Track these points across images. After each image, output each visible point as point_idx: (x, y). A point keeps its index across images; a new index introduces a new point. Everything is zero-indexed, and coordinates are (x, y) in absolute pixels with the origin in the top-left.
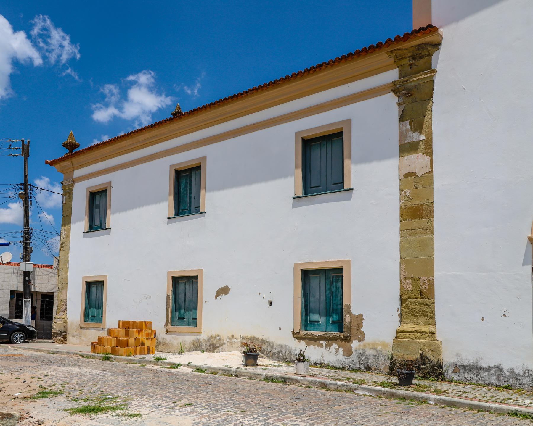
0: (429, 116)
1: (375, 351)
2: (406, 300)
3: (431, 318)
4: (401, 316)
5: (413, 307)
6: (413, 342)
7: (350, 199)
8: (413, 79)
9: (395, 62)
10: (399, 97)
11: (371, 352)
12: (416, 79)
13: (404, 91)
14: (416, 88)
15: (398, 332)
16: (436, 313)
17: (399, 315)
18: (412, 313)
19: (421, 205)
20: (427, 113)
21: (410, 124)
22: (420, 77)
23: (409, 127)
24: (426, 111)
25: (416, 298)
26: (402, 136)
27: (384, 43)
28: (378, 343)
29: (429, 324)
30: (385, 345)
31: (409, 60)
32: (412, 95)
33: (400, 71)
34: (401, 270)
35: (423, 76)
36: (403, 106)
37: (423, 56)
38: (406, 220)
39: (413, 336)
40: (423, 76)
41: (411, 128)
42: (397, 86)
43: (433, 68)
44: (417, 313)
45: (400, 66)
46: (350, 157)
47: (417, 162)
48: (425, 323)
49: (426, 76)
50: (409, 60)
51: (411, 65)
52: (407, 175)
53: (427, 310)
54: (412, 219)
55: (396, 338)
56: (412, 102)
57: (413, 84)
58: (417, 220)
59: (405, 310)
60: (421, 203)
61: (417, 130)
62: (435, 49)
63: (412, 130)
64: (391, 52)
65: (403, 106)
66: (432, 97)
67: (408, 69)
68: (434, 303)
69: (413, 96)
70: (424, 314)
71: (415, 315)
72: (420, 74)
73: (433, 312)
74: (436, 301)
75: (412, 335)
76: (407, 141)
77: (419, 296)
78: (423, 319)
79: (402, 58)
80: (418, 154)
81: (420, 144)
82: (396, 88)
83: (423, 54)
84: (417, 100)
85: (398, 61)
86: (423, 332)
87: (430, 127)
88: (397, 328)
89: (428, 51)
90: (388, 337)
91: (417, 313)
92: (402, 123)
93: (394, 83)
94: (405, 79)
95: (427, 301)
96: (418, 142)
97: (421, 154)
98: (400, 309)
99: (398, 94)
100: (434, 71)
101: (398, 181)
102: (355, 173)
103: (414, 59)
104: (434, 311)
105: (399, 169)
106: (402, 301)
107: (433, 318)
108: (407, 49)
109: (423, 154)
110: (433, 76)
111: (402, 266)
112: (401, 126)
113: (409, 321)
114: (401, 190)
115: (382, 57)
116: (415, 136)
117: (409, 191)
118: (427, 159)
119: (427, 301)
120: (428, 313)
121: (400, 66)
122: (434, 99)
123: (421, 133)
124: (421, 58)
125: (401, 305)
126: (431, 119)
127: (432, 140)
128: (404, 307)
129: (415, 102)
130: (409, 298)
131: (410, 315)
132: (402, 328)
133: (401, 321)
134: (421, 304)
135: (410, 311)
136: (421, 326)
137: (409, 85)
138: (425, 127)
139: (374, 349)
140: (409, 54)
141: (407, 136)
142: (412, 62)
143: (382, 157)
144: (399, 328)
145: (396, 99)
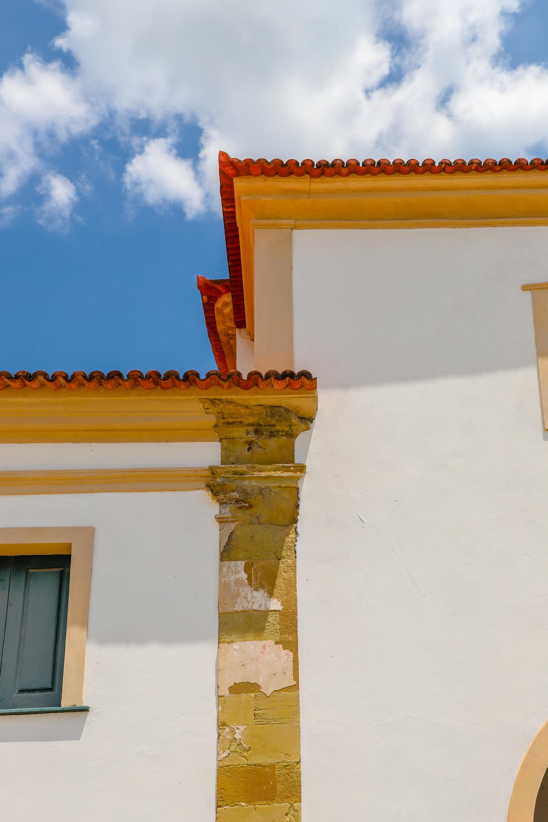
0: (290, 561)
7: (76, 736)
8: (257, 474)
9: (216, 426)
10: (222, 503)
12: (263, 474)
13: (235, 495)
14: (261, 493)
19: (272, 766)
20: (284, 553)
21: (247, 569)
22: (272, 473)
23: (244, 576)
24: (282, 549)
26: (226, 592)
27: (203, 376)
31: (248, 433)
32: (250, 507)
33: (224, 449)
35: (279, 474)
36: (231, 527)
37: (278, 432)
38: (234, 803)
40: (279, 474)
41: (249, 579)
42: (219, 480)
43: (297, 461)
45: (226, 438)
46: (85, 623)
47: (260, 659)
49: (285, 474)
50: (248, 433)
51: (250, 444)
52: (237, 689)
54: (249, 802)
56: (252, 523)
57: (254, 483)
58: (262, 806)
60: (270, 761)
61: (262, 586)
62: (303, 426)
63: (250, 583)
64: (212, 401)
65: (231, 527)
66: (296, 522)
67: (242, 450)
69: (254, 509)
72: (275, 466)
76: (238, 608)
79: (233, 423)
80: (263, 643)
81: (270, 619)
82: (215, 484)
83: (278, 428)
84: (262, 520)
85: (223, 427)
87: (292, 584)
89: (290, 426)
92: (227, 563)
93: (213, 470)
94: (242, 468)
96: (265, 614)
97: (270, 643)
99: (221, 496)
100: (302, 468)
101: (214, 699)
102: (95, 665)
103: (257, 432)
105: (218, 671)
108: (246, 407)
109: (277, 643)
110: (298, 478)
112: (225, 569)
114: (221, 725)
115: (189, 406)
116: (257, 600)
117: (242, 728)
118: (286, 656)
121: (226, 438)
122: (300, 525)
123: (271, 594)
124: (272, 435)
126: (293, 568)
127: (295, 613)
129: (258, 522)
137: (246, 483)
138: (279, 581)
140: (251, 420)
141: (239, 595)
142: (252, 437)
143: (174, 634)
145: (214, 508)
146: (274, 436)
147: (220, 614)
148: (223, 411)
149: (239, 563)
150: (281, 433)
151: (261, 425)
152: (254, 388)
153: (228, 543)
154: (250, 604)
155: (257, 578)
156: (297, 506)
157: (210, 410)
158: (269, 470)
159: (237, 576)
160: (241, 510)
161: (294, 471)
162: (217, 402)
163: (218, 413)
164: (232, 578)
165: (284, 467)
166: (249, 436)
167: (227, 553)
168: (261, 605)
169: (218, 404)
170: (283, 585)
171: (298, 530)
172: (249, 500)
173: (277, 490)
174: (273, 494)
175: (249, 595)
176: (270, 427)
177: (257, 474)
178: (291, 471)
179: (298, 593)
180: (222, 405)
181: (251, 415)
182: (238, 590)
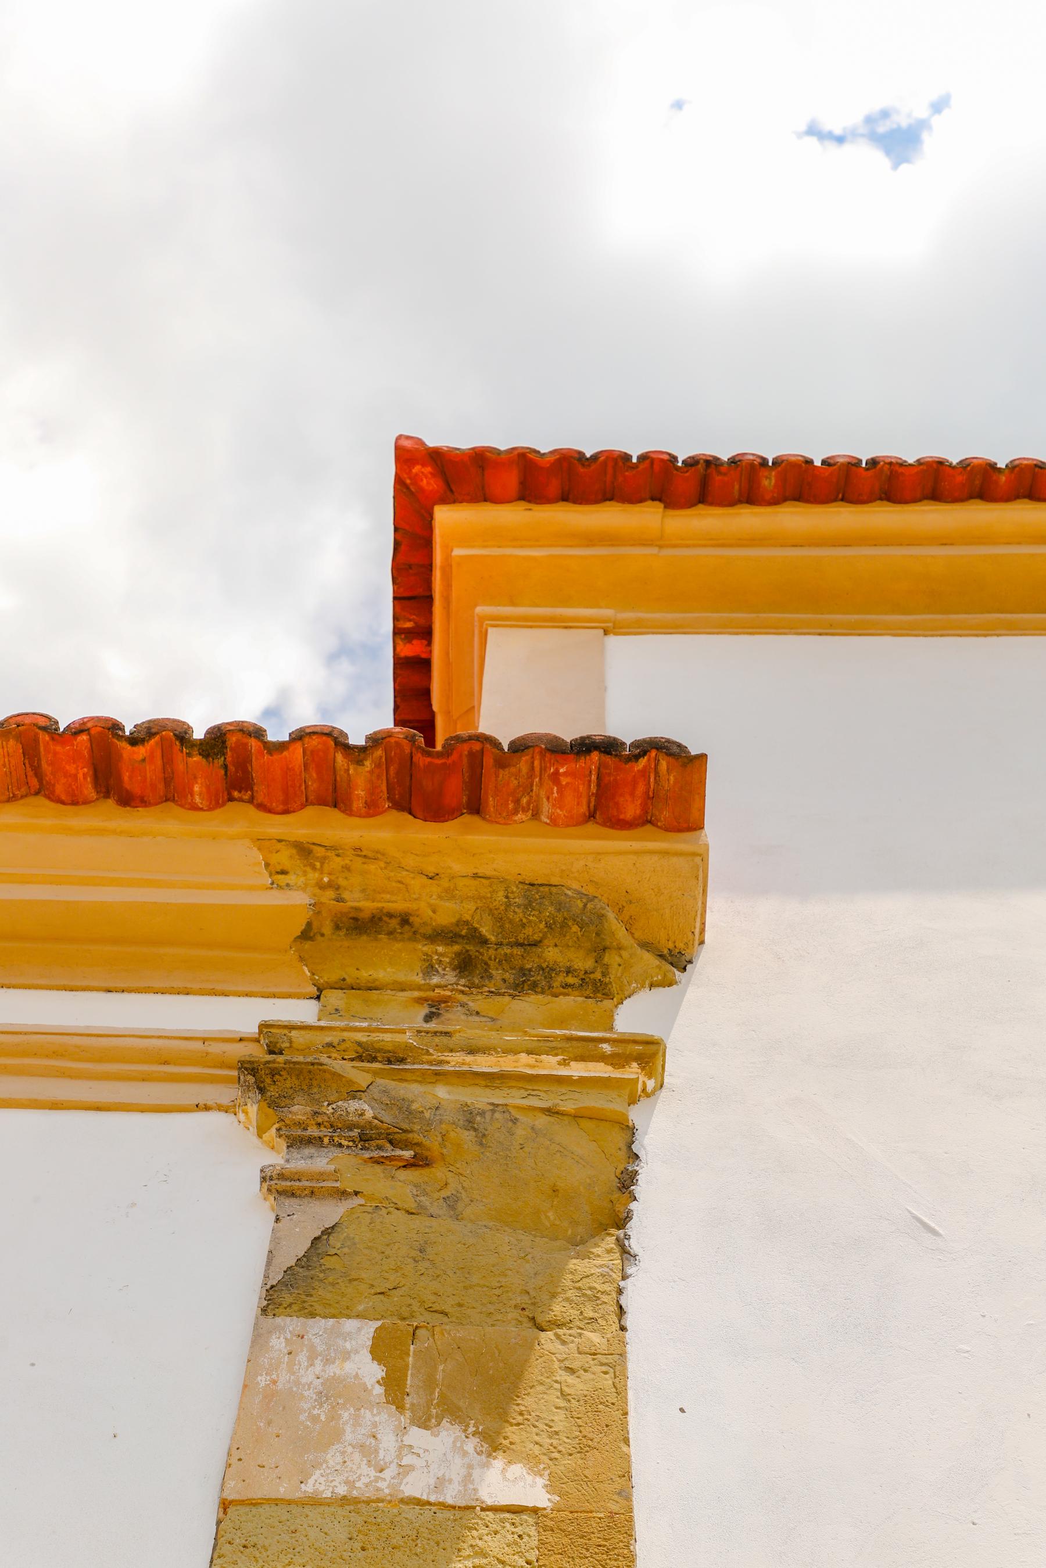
21: (382, 1349)
23: (372, 1372)
31: (430, 969)
32: (421, 1161)
37: (549, 971)
45: (342, 985)
49: (577, 1070)
50: (430, 969)
61: (453, 1412)
64: (304, 850)
69: (438, 1172)
76: (321, 1483)
83: (552, 954)
89: (600, 950)
92: (291, 1324)
99: (299, 1110)
103: (464, 965)
112: (278, 1343)
124: (524, 983)
127: (621, 1525)
146: (534, 987)
147: (225, 1505)
148: (342, 882)
149: (350, 1325)
150: (561, 979)
151: (485, 942)
152: (467, 818)
153: (305, 1261)
154: (387, 1474)
155: (430, 1383)
156: (627, 1182)
157: (291, 879)
158: (511, 1050)
159: (333, 1370)
160: (378, 1168)
161: (617, 1060)
162: (319, 852)
163: (322, 887)
164: (310, 1375)
165: (570, 1039)
166: (435, 980)
167: (293, 1290)
168: (440, 1483)
169: (323, 860)
170: (559, 1417)
171: (634, 1245)
172: (415, 1137)
173: (542, 1121)
174: (520, 1132)
175: (388, 1442)
176: (518, 951)
177: (456, 1061)
178: (603, 1058)
179: (635, 1450)
180: (337, 862)
181: (450, 894)
182: (333, 1417)
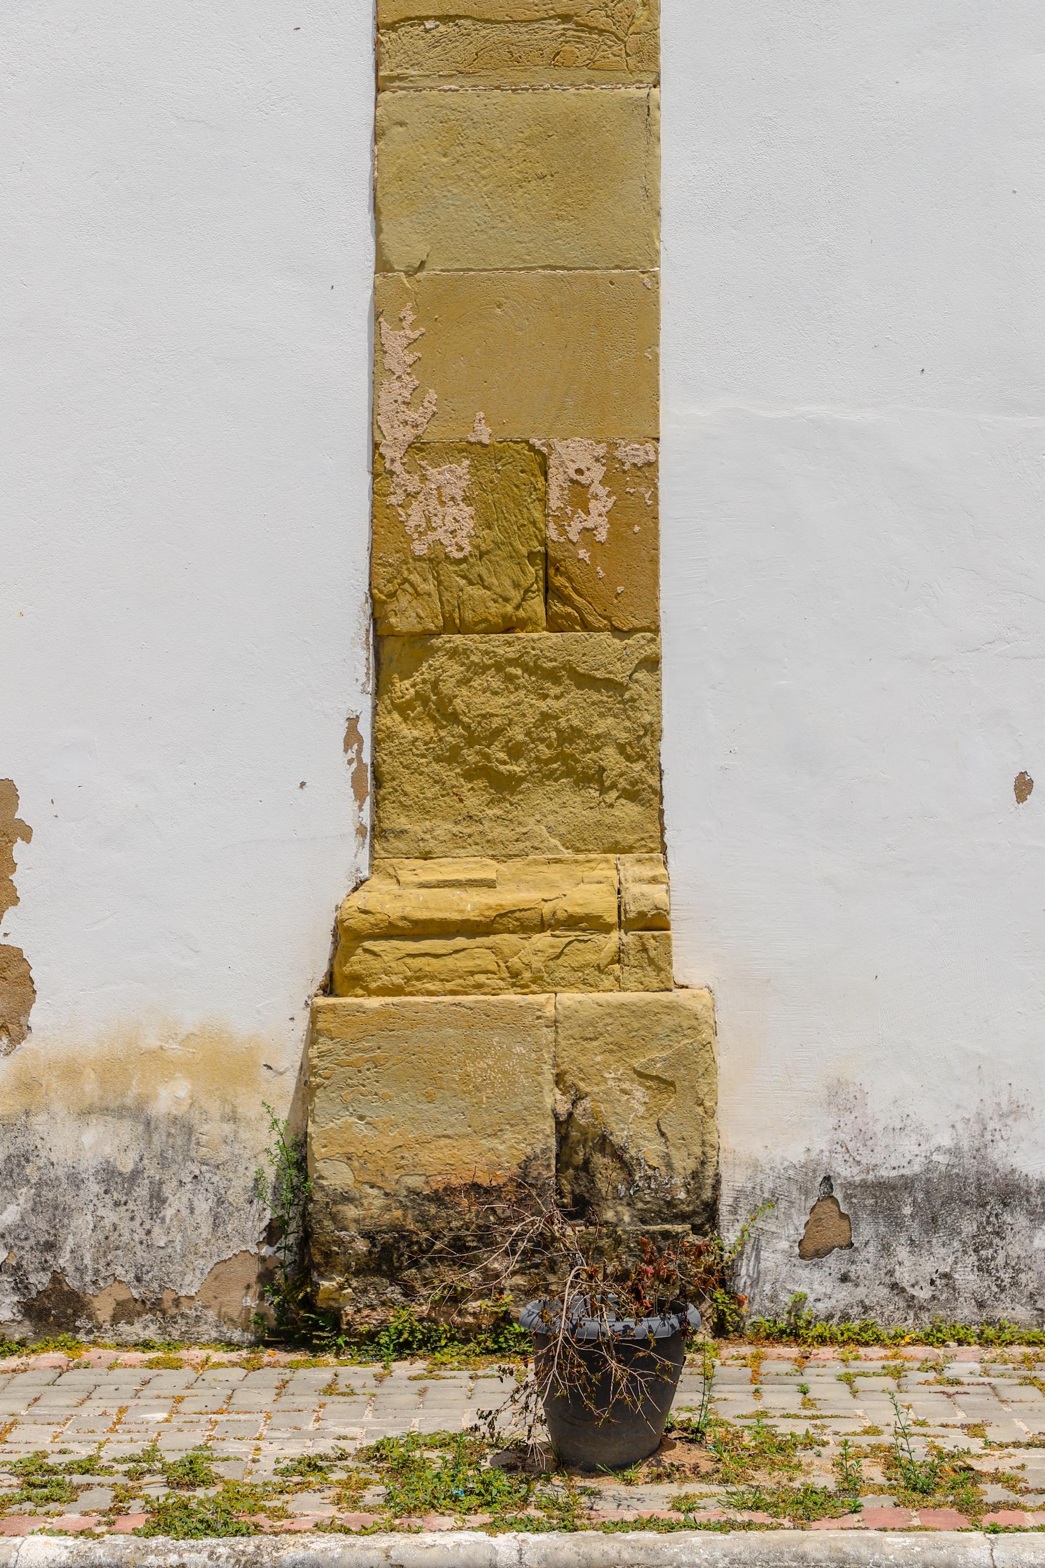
1: (126, 1130)
2: (420, 642)
3: (631, 795)
4: (376, 783)
5: (478, 700)
6: (490, 1017)
11: (97, 1144)
15: (346, 937)
16: (670, 752)
17: (357, 781)
18: (471, 756)
25: (509, 626)
28: (155, 1055)
29: (616, 848)
30: (226, 1065)
34: (379, 372)
39: (488, 961)
44: (515, 752)
48: (579, 842)
53: (602, 726)
55: (329, 988)
59: (407, 732)
68: (652, 664)
70: (570, 762)
71: (492, 769)
73: (643, 744)
74: (671, 646)
75: (477, 953)
77: (536, 605)
78: (561, 806)
86: (572, 922)
88: (338, 891)
90: (257, 994)
91: (515, 752)
95: (600, 651)
98: (365, 729)
104: (653, 731)
106: (391, 649)
107: (647, 795)
111: (395, 341)
113: (444, 828)
119: (600, 651)
120: (610, 757)
125: (378, 692)
128: (403, 709)
130: (451, 626)
131: (450, 774)
132: (387, 900)
133: (377, 833)
134: (553, 676)
135: (452, 735)
136: (553, 872)
139: (121, 1112)
144: (358, 900)
